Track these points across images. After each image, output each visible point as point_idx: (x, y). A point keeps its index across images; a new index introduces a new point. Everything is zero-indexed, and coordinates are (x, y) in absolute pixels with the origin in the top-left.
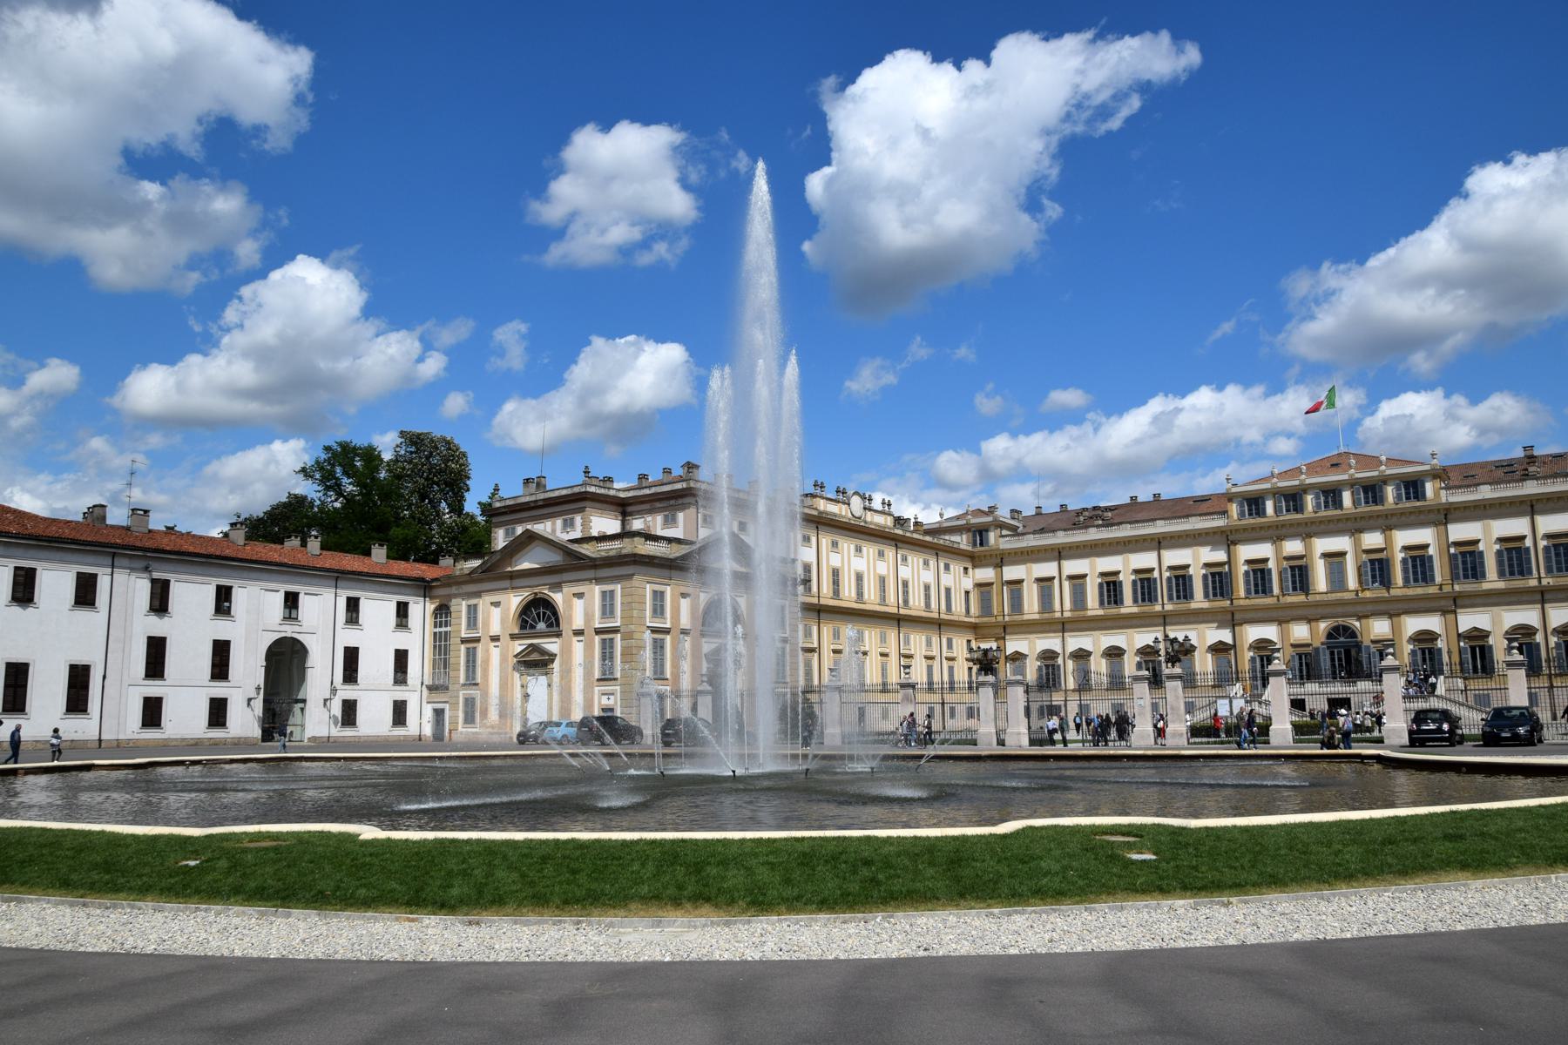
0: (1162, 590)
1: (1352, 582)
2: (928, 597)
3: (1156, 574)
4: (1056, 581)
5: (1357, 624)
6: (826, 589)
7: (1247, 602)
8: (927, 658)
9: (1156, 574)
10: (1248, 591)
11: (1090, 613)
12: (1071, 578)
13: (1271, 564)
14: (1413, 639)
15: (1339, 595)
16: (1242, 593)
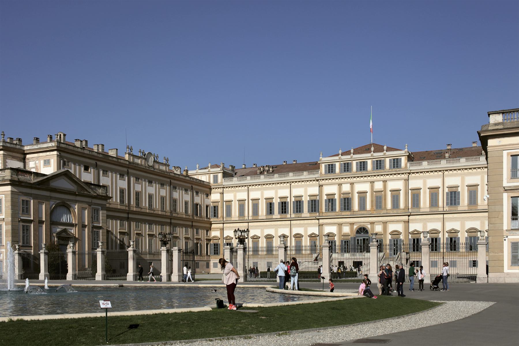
0: (291, 207)
1: (368, 207)
2: (186, 208)
3: (289, 200)
4: (246, 202)
5: (369, 226)
6: (133, 202)
7: (325, 214)
8: (186, 238)
9: (289, 200)
10: (325, 210)
11: (260, 218)
12: (252, 200)
13: (336, 197)
14: (391, 234)
15: (363, 212)
16: (324, 210)
